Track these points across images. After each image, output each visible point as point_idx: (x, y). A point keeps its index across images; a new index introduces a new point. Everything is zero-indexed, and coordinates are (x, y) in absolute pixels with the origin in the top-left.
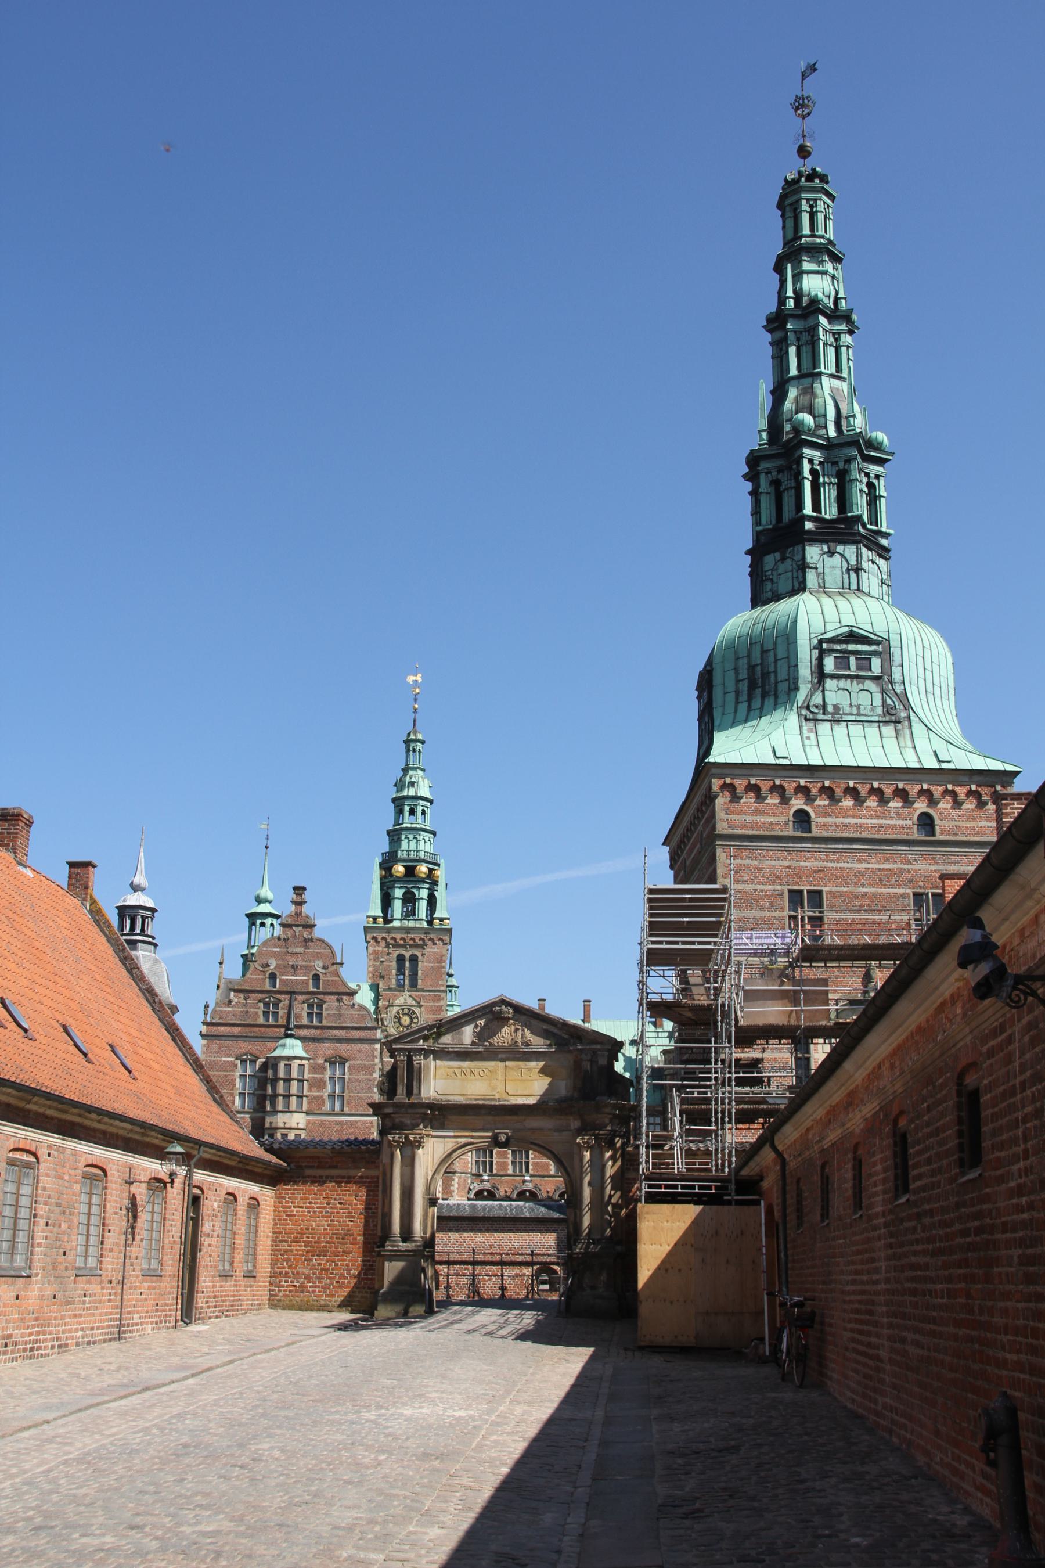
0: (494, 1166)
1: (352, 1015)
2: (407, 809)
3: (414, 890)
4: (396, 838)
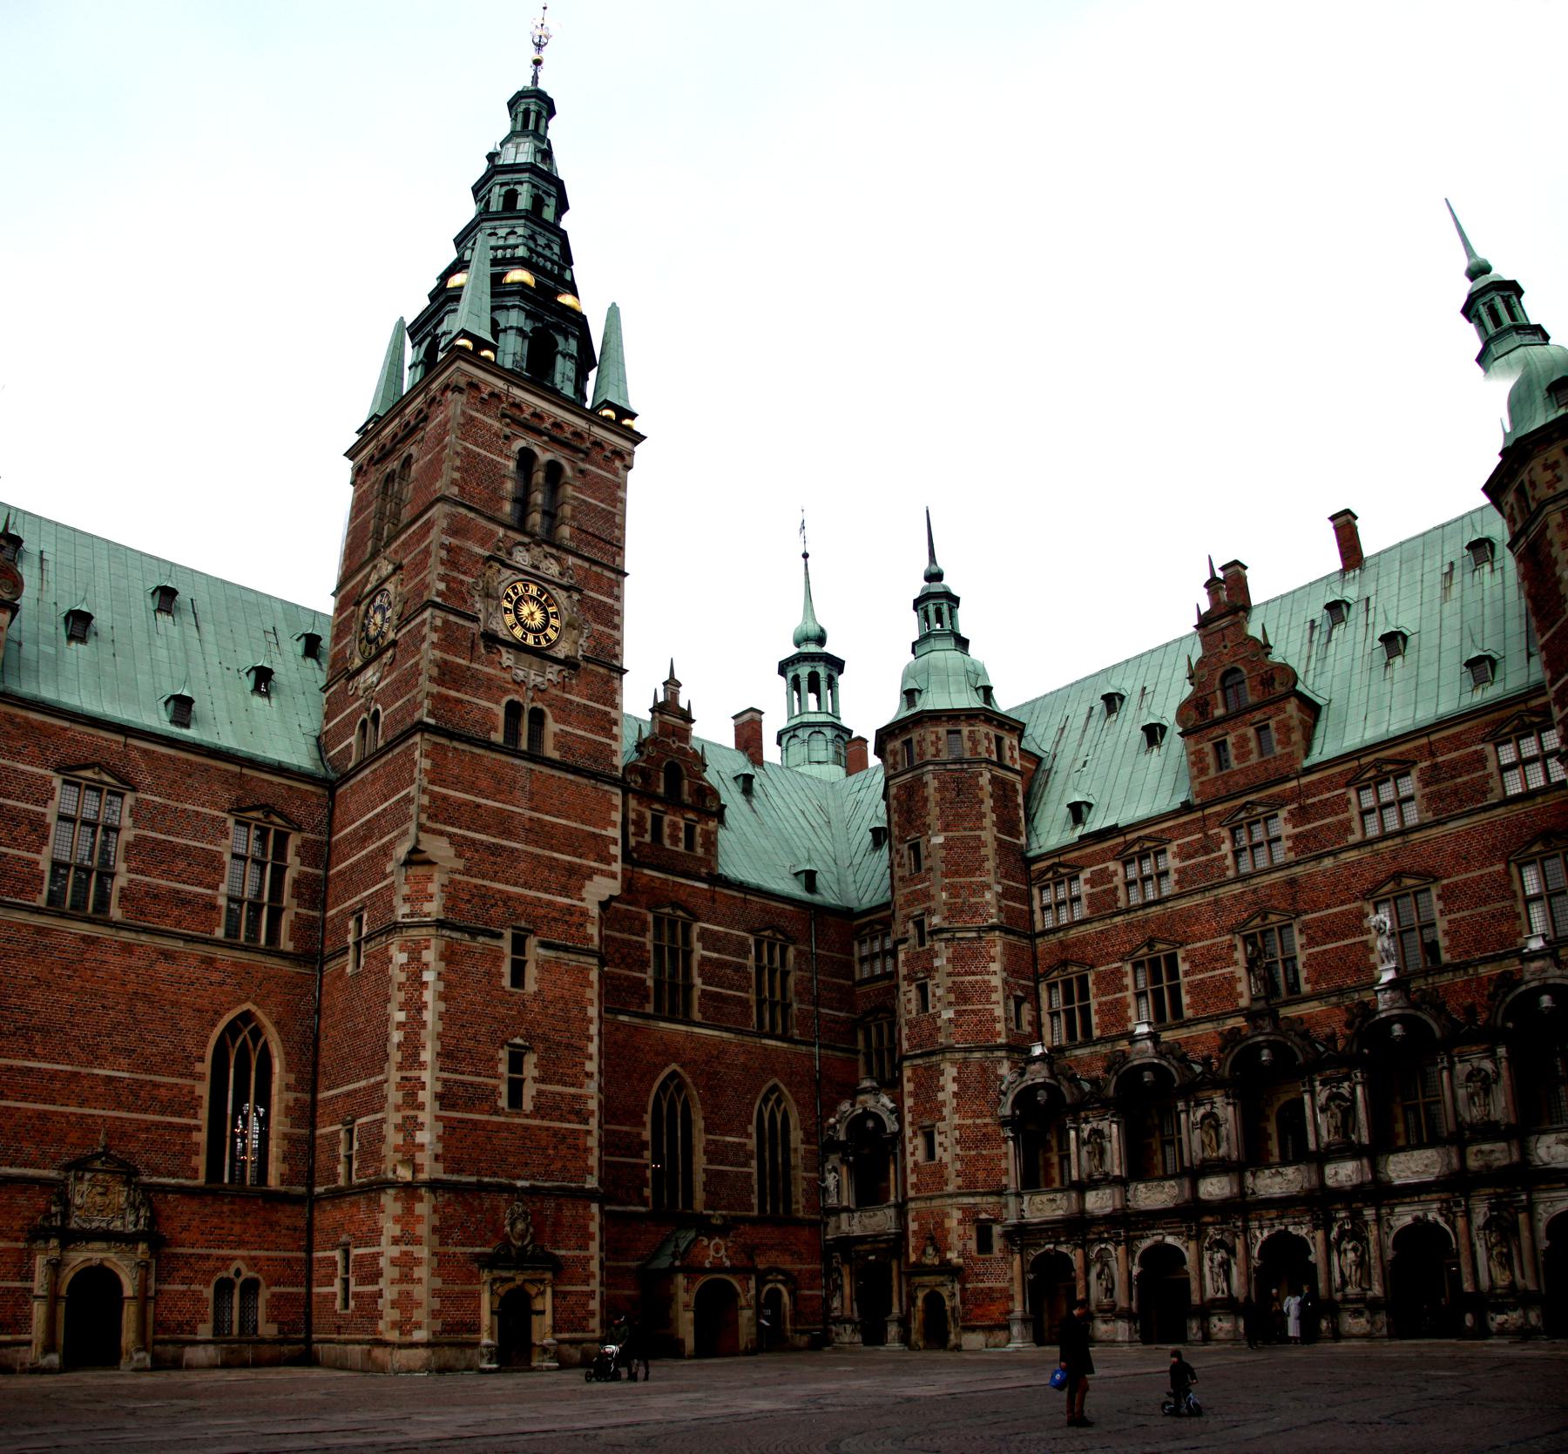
0: (1095, 1019)
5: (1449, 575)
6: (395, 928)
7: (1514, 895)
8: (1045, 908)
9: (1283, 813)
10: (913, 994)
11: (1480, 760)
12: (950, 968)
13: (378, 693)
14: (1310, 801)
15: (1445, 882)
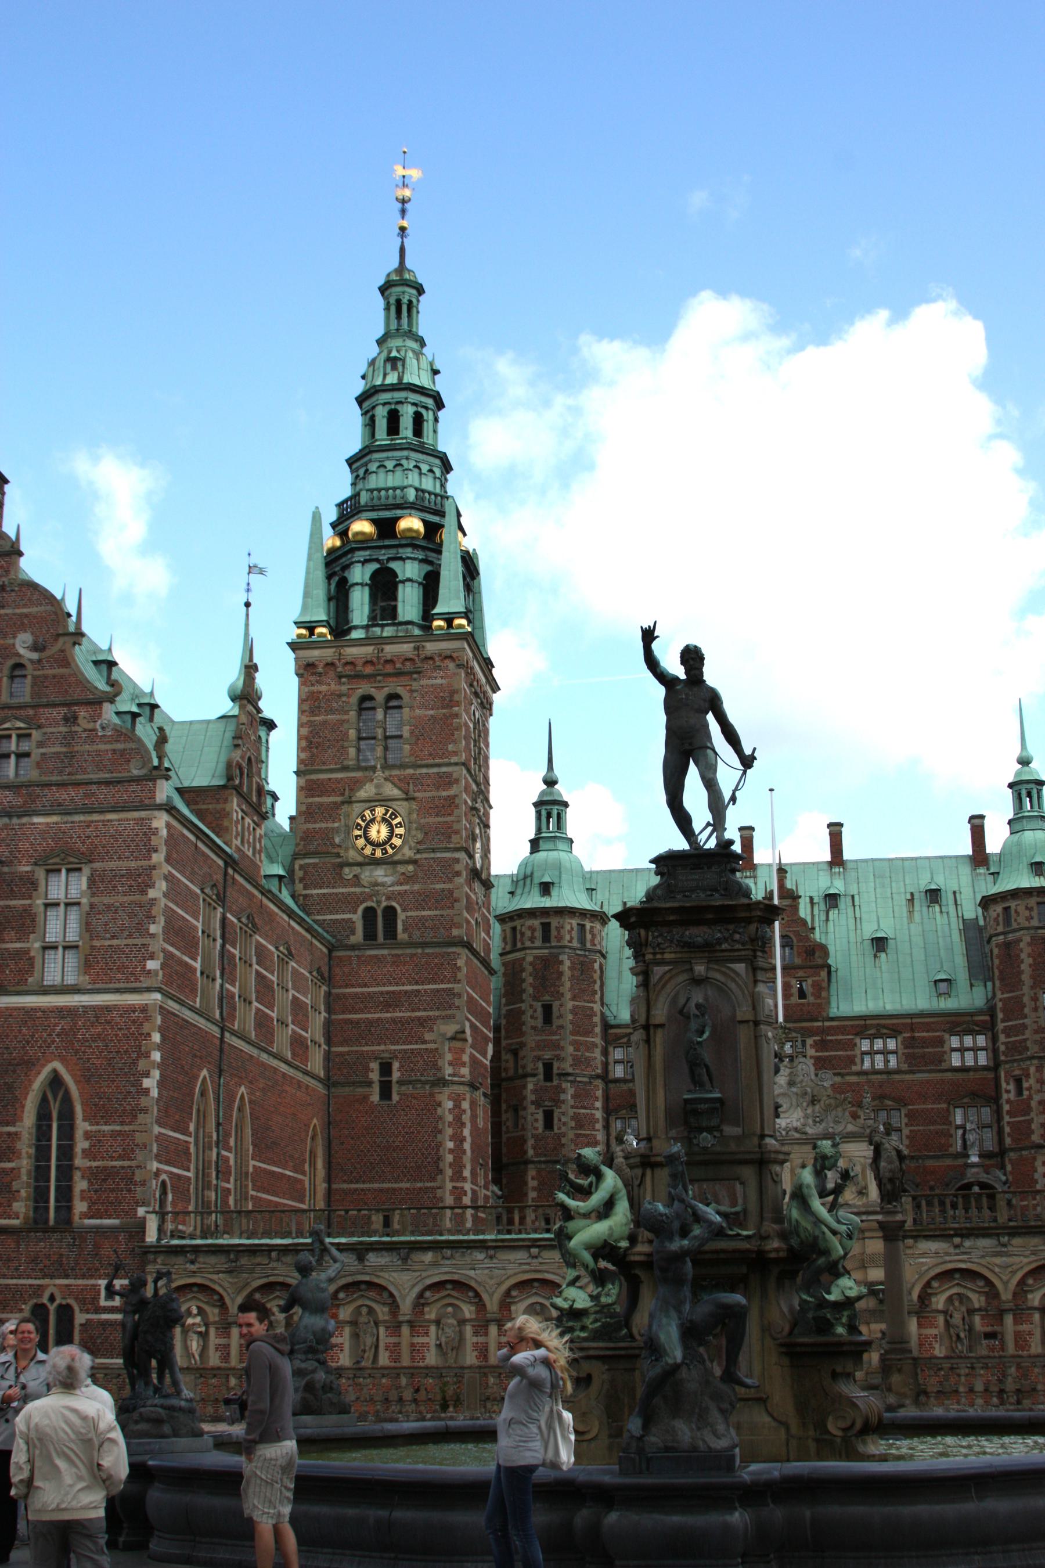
1: (98, 753)
2: (381, 413)
3: (393, 565)
4: (361, 472)
5: (911, 901)
6: (442, 1082)
7: (950, 1123)
8: (616, 1062)
9: (809, 1041)
10: (540, 1116)
11: (941, 1042)
12: (572, 1102)
13: (393, 892)
14: (829, 1038)
15: (910, 1107)
